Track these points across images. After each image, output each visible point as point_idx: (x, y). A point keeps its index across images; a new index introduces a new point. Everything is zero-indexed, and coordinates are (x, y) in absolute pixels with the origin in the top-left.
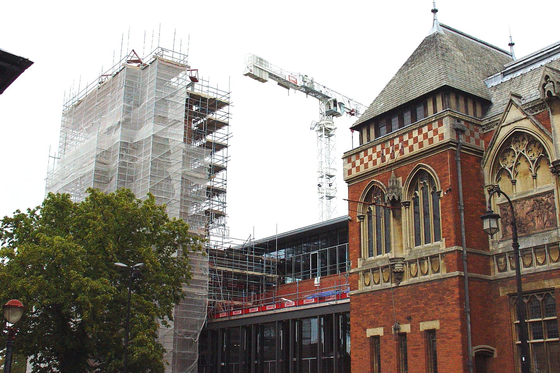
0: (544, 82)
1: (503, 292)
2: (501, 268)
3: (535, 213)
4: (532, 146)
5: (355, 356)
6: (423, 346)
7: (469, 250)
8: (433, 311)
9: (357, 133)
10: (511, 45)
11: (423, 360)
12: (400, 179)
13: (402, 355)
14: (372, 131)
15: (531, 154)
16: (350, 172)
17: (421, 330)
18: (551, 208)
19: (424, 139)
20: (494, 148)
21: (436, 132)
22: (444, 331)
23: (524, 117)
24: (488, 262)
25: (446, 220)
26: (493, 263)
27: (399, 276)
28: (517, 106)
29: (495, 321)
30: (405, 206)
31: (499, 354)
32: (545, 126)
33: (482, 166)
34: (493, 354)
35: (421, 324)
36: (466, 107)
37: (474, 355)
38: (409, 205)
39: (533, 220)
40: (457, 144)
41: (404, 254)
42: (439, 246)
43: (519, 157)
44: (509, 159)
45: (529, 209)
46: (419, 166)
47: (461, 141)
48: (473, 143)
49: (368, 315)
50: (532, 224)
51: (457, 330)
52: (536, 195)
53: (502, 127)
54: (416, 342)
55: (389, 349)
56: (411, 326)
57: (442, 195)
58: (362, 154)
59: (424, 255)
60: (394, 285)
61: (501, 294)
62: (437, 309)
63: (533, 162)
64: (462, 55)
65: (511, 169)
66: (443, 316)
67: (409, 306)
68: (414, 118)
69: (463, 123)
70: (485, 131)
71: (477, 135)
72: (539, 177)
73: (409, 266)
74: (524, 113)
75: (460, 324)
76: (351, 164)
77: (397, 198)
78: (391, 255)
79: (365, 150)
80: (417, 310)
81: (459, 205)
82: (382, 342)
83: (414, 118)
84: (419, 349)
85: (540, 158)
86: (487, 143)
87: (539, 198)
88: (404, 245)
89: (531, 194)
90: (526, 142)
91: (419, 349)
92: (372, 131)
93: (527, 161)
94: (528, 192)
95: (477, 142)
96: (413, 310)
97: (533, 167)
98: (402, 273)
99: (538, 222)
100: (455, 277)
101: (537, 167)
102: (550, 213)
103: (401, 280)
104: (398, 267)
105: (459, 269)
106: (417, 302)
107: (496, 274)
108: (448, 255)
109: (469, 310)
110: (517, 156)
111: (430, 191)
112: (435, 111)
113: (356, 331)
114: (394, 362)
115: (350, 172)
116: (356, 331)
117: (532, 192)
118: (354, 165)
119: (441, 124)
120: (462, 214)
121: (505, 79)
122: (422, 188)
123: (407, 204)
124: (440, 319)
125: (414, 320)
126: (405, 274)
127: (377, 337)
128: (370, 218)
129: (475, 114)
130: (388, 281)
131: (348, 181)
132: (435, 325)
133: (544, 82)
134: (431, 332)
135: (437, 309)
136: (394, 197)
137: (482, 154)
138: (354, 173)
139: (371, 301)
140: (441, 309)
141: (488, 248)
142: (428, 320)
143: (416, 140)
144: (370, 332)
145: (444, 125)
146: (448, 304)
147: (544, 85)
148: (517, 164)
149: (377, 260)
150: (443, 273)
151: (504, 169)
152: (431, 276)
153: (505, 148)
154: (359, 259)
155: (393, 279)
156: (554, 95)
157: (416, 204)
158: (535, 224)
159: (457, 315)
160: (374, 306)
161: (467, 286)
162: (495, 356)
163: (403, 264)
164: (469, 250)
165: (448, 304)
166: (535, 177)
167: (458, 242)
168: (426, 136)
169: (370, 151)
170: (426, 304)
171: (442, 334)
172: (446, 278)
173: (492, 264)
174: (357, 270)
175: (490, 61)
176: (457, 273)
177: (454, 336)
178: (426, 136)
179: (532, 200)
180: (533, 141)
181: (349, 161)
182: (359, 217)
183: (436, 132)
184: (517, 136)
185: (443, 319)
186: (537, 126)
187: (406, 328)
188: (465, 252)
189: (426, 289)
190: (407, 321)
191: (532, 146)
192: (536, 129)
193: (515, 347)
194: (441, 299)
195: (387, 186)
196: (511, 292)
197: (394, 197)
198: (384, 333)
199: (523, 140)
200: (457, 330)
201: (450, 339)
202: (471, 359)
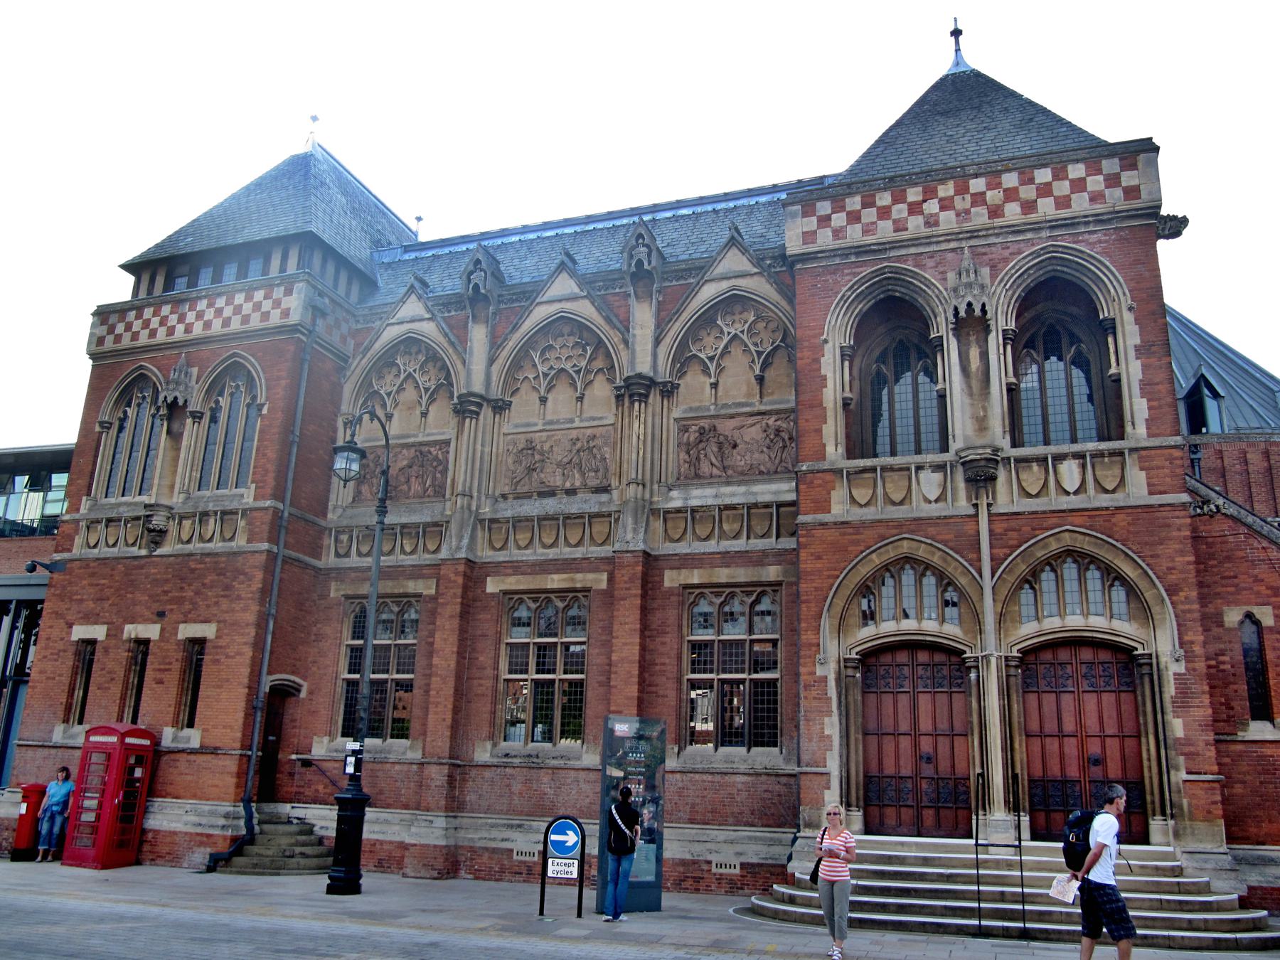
0: (471, 267)
1: (337, 590)
2: (342, 551)
3: (413, 471)
4: (430, 365)
5: (41, 672)
6: (177, 666)
7: (293, 511)
8: (208, 606)
9: (131, 279)
10: (419, 219)
11: (174, 691)
12: (195, 370)
13: (134, 680)
14: (160, 281)
15: (426, 378)
16: (101, 341)
17: (181, 636)
18: (440, 468)
19: (254, 311)
20: (369, 355)
21: (277, 304)
22: (222, 642)
23: (427, 316)
24: (321, 539)
25: (264, 455)
26: (329, 542)
27: (158, 536)
28: (420, 297)
29: (313, 637)
30: (194, 417)
31: (310, 692)
32: (458, 337)
33: (343, 381)
34: (299, 691)
35: (182, 626)
36: (336, 280)
37: (267, 690)
38: (201, 418)
39: (408, 481)
40: (310, 332)
41: (175, 500)
42: (242, 496)
43: (406, 379)
44: (389, 378)
45: (405, 463)
46: (235, 355)
48: (335, 339)
49: (81, 601)
50: (405, 487)
51: (245, 644)
52: (421, 444)
53: (388, 325)
55: (111, 666)
56: (162, 630)
57: (265, 411)
58: (132, 314)
59: (211, 507)
60: (144, 552)
61: (332, 595)
63: (427, 390)
64: (344, 200)
65: (389, 394)
66: (227, 617)
67: (166, 592)
68: (242, 273)
69: (327, 301)
70: (359, 326)
71: (344, 328)
72: (431, 416)
73: (180, 524)
74: (429, 311)
75: (253, 634)
76: (105, 328)
77: (181, 402)
78: (145, 499)
79: (140, 310)
80: (179, 601)
81: (293, 432)
82: (99, 654)
83: (242, 273)
84: (169, 670)
85: (439, 387)
86: (358, 345)
87: (425, 449)
88: (177, 486)
89: (412, 440)
90: (422, 358)
91: (169, 670)
92: (160, 281)
93: (417, 387)
94: (408, 436)
95: (343, 339)
96: (171, 601)
97: (425, 399)
98: (162, 533)
99: (416, 487)
100: (262, 552)
101: (432, 400)
102: (438, 475)
103: (158, 544)
104: (158, 521)
105: (269, 541)
106: (182, 588)
107: (329, 560)
108: (255, 514)
109: (273, 611)
110: (402, 376)
111: (244, 400)
112: (283, 269)
113: (51, 627)
114: (116, 689)
115: (101, 341)
116: (51, 627)
117: (415, 436)
118: (111, 330)
119: (289, 292)
120: (295, 450)
121: (406, 257)
122: (232, 395)
123: (198, 416)
124: (219, 622)
125: (170, 617)
126: (169, 534)
127: (92, 642)
128: (121, 429)
129: (348, 294)
130: (133, 544)
131: (93, 356)
132: (207, 631)
133: (471, 267)
135: (217, 603)
136: (176, 398)
137: (346, 361)
138: (109, 344)
139: (93, 575)
140: (225, 604)
141: (325, 515)
142: (195, 622)
143: (238, 310)
144: (80, 632)
145: (295, 295)
146: (239, 598)
147: (471, 273)
148: (401, 389)
149: (120, 505)
150: (241, 542)
151: (376, 392)
152: (217, 546)
153: (386, 361)
154: (84, 498)
155: (144, 541)
156: (483, 291)
157: (214, 420)
158: (410, 489)
159: (251, 617)
161: (278, 570)
162: (303, 694)
163: (168, 518)
164: (293, 511)
165: (239, 598)
166: (424, 414)
167: (279, 495)
168: (257, 307)
169: (148, 313)
170: (197, 593)
172: (244, 553)
173: (326, 542)
174: (77, 516)
175: (384, 228)
176: (265, 546)
178: (257, 307)
179: (413, 450)
180: (433, 357)
182: (101, 424)
183: (277, 304)
184: (410, 344)
185: (225, 621)
186: (446, 335)
188: (286, 514)
190: (156, 618)
191: (430, 365)
192: (441, 339)
193: (340, 683)
194: (227, 587)
195: (166, 377)
196: (350, 592)
197: (176, 398)
198: (108, 635)
199: (417, 353)
200: (245, 644)
201: (233, 657)
202: (261, 695)
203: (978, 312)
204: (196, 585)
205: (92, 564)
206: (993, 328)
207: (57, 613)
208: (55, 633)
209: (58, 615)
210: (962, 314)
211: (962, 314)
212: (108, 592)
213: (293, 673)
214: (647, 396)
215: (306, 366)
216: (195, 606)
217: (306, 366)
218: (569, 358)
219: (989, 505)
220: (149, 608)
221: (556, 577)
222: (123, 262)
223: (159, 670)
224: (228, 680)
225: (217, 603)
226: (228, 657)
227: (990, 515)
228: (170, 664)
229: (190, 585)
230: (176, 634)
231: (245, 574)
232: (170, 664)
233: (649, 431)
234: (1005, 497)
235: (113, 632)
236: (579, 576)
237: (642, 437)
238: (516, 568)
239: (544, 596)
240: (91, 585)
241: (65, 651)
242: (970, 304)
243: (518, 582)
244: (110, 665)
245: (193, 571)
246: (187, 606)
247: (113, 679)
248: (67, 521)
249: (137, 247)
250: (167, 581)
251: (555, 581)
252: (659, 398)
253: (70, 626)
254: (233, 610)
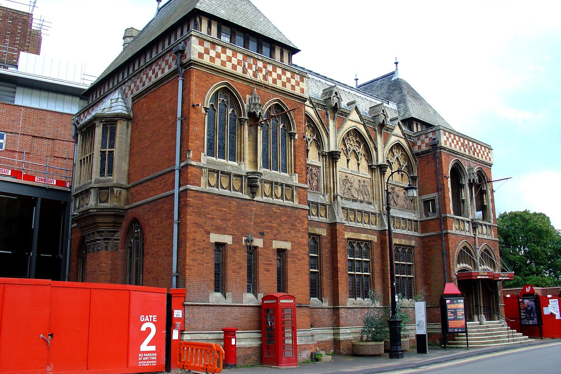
22: (296, 252)
35: (274, 242)
51: (305, 254)
54: (268, 258)
56: (264, 242)
62: (289, 232)
66: (295, 239)
67: (263, 222)
80: (271, 228)
82: (229, 252)
84: (270, 264)
91: (270, 264)
96: (267, 227)
106: (270, 221)
113: (195, 232)
124: (292, 242)
127: (223, 245)
132: (286, 245)
134: (281, 252)
139: (217, 204)
140: (293, 233)
144: (215, 238)
146: (299, 231)
160: (222, 211)
171: (293, 254)
172: (299, 208)
177: (303, 258)
187: (258, 242)
189: (279, 211)
190: (259, 235)
194: (293, 225)
200: (305, 254)
204: (278, 221)
205: (215, 197)
207: (197, 224)
208: (198, 236)
209: (198, 225)
212: (229, 216)
216: (279, 232)
220: (255, 229)
223: (267, 264)
224: (300, 271)
225: (289, 232)
226: (298, 260)
228: (271, 261)
229: (275, 220)
230: (272, 246)
231: (300, 219)
232: (271, 261)
235: (236, 240)
236: (369, 236)
238: (352, 229)
239: (357, 242)
240: (217, 210)
241: (207, 248)
243: (352, 235)
244: (238, 259)
245: (275, 213)
246: (275, 232)
247: (241, 267)
248: (194, 166)
250: (262, 216)
251: (363, 237)
253: (208, 233)
254: (298, 237)
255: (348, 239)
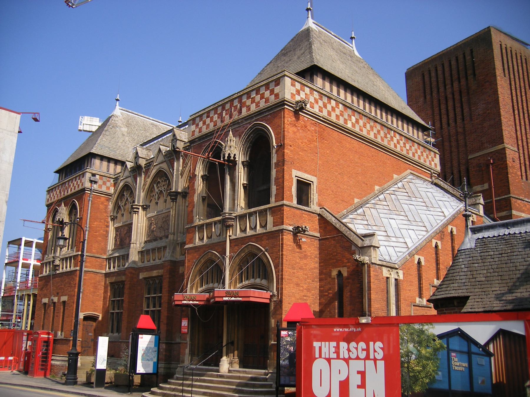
40: (91, 189)
47: (93, 188)
48: (104, 189)
94: (127, 221)
104: (57, 262)
124: (68, 295)
125: (60, 294)
134: (64, 302)
170: (65, 286)
181: (49, 194)
193: (110, 314)
194: (70, 284)
203: (232, 158)
206: (237, 162)
210: (226, 158)
211: (226, 158)
213: (94, 311)
214: (176, 199)
215: (90, 202)
217: (90, 202)
218: (164, 185)
219: (230, 236)
221: (155, 271)
222: (55, 171)
227: (230, 240)
233: (177, 213)
234: (235, 232)
237: (174, 216)
242: (229, 154)
249: (59, 166)
251: (155, 273)
252: (181, 199)
255: (145, 278)
